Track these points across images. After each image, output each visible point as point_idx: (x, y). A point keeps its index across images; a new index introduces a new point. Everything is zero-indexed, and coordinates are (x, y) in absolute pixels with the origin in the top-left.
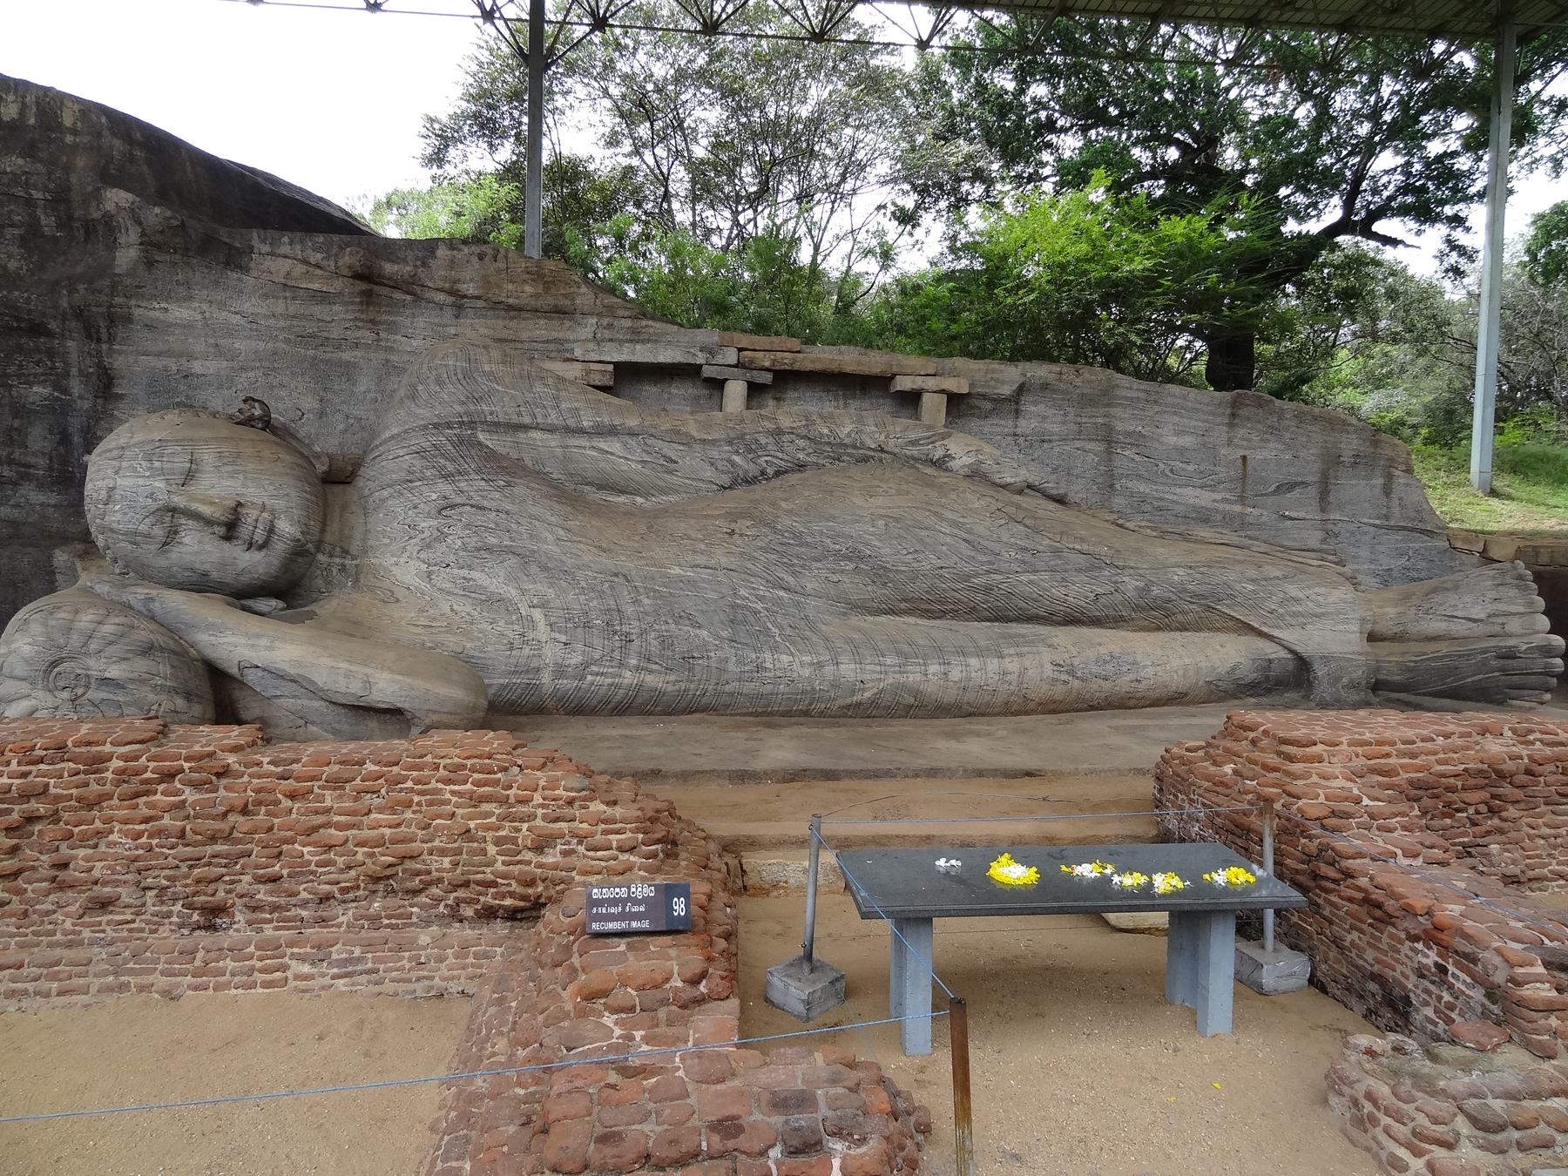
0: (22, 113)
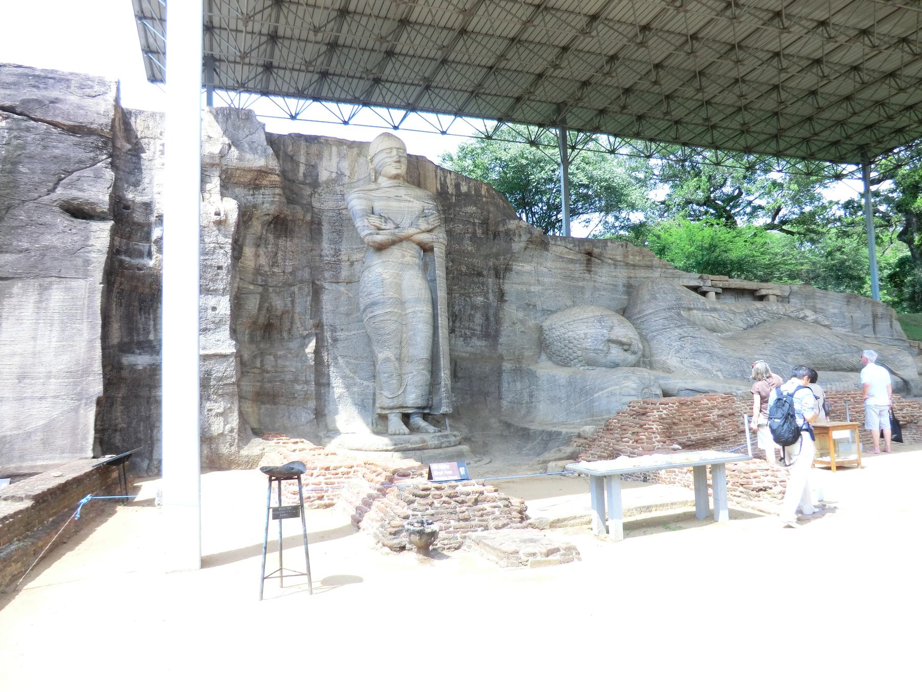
0: (469, 188)
